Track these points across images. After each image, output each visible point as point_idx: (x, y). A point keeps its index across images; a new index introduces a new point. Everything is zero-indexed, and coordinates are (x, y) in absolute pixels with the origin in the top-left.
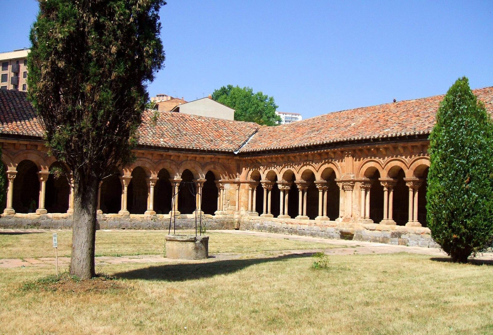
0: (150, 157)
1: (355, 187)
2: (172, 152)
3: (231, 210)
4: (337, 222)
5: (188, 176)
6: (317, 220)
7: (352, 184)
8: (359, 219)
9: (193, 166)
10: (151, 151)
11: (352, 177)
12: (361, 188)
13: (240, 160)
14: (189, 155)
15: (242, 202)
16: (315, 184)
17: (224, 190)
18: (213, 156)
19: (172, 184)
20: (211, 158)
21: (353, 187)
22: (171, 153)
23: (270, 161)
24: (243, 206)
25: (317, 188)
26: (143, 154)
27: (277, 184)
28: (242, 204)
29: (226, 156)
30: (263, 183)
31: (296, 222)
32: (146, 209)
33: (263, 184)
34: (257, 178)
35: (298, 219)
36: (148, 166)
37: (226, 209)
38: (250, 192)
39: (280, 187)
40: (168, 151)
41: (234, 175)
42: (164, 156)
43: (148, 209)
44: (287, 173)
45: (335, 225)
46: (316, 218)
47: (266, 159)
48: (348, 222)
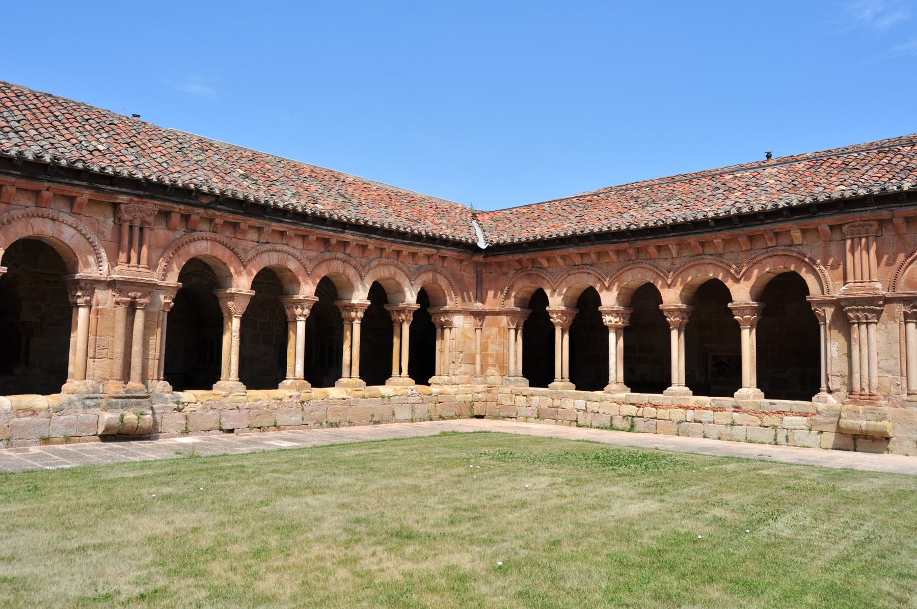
0: (298, 243)
1: (884, 314)
2: (352, 234)
3: (465, 374)
4: (820, 404)
5: (378, 293)
6: (741, 397)
7: (880, 306)
8: (905, 397)
9: (393, 272)
10: (304, 228)
11: (880, 289)
12: (906, 316)
13: (485, 265)
14: (386, 245)
15: (492, 355)
16: (730, 310)
17: (453, 330)
18: (434, 251)
19: (344, 314)
20: (429, 257)
21: (879, 314)
22: (349, 236)
23: (578, 261)
24: (494, 366)
25: (736, 322)
26: (282, 234)
27: (599, 315)
28: (491, 360)
29: (460, 252)
30: (554, 312)
31: (669, 402)
32: (283, 377)
33: (554, 316)
34: (538, 300)
35: (672, 394)
36: (292, 265)
37: (456, 373)
38: (513, 332)
39: (608, 320)
40: (343, 232)
41: (465, 294)
42: (333, 241)
43: (289, 374)
44: (627, 288)
45: (813, 411)
46: (736, 394)
47: (564, 257)
48: (872, 404)
